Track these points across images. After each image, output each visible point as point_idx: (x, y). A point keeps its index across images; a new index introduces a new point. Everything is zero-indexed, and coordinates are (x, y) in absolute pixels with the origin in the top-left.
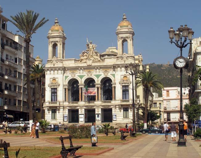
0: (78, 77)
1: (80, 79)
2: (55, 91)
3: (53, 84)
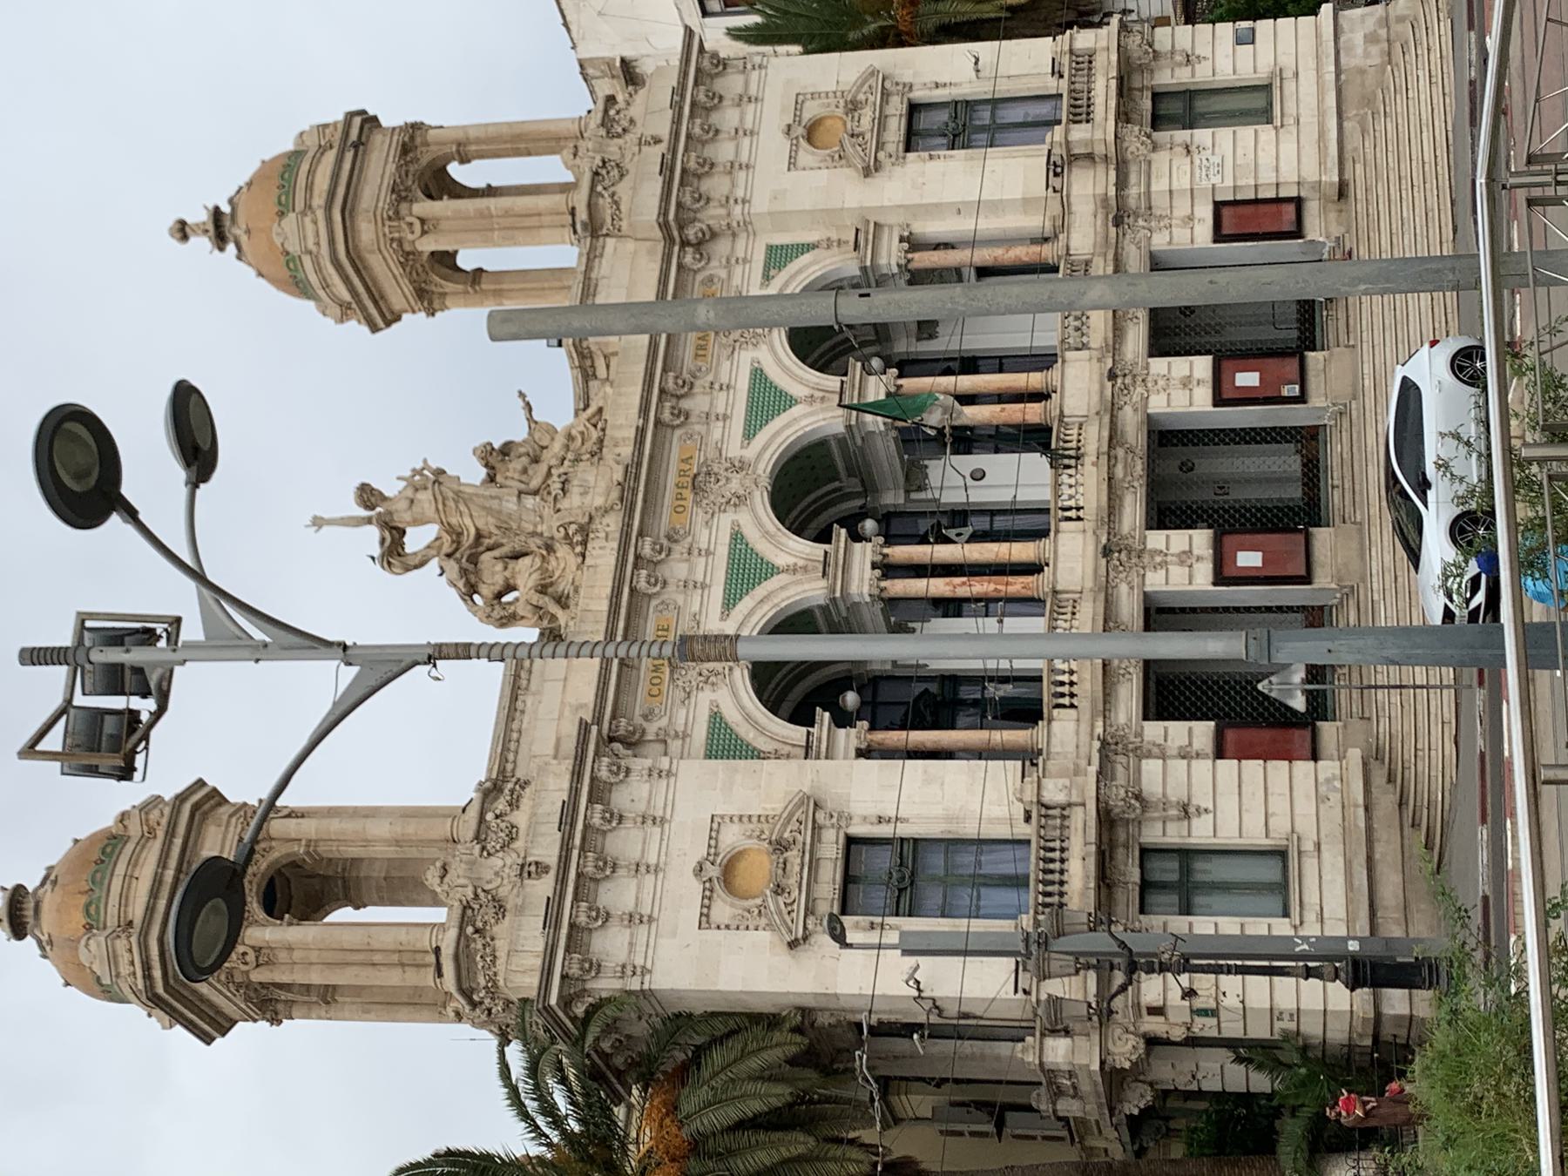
0: (746, 604)
2: (883, 861)
3: (792, 881)
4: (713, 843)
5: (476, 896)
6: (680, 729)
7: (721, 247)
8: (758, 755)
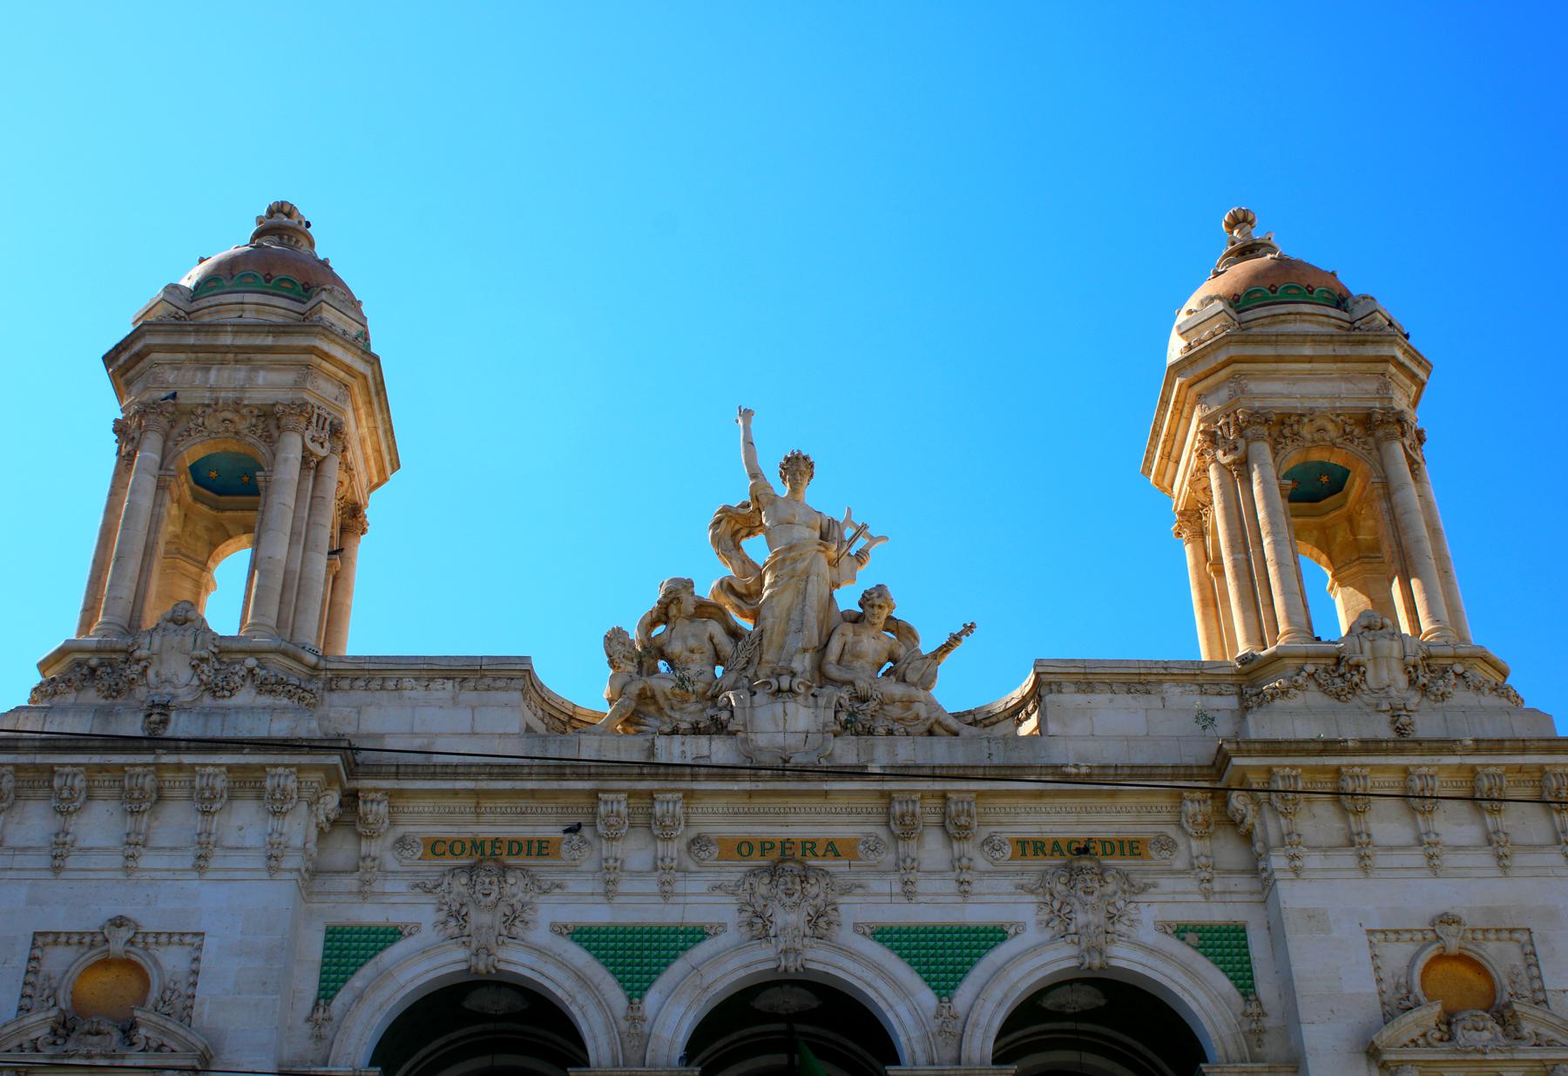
0: (579, 956)
1: (616, 997)
4: (163, 939)
5: (138, 661)
6: (377, 887)
7: (1228, 851)
8: (327, 991)
